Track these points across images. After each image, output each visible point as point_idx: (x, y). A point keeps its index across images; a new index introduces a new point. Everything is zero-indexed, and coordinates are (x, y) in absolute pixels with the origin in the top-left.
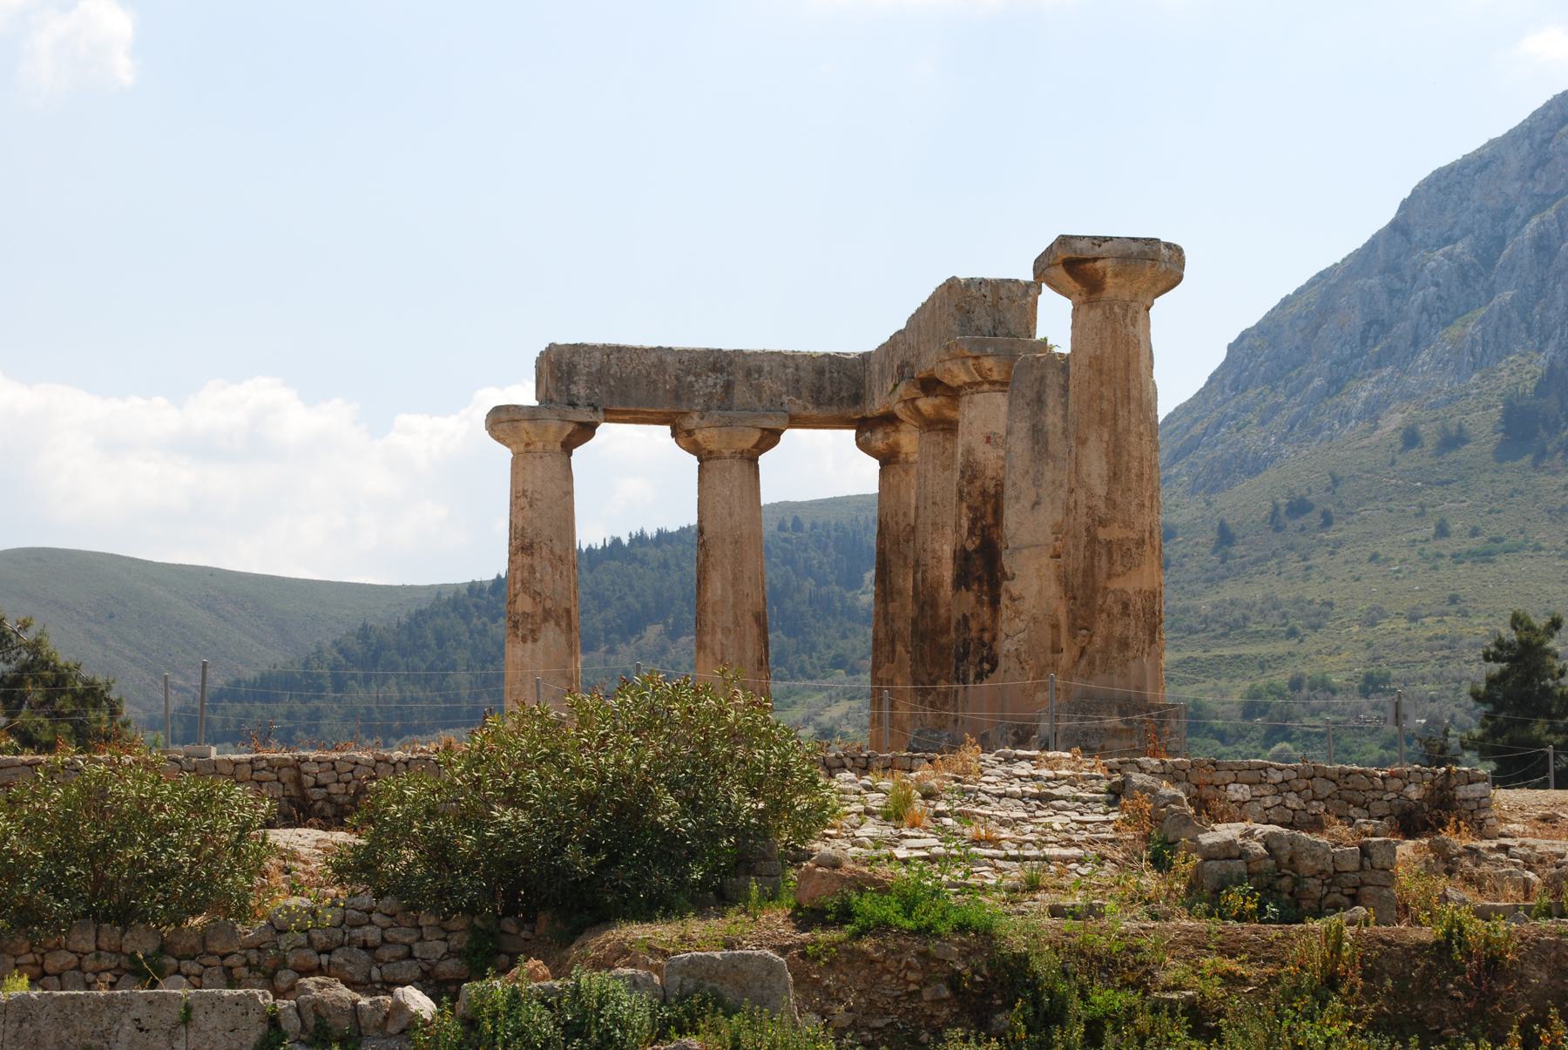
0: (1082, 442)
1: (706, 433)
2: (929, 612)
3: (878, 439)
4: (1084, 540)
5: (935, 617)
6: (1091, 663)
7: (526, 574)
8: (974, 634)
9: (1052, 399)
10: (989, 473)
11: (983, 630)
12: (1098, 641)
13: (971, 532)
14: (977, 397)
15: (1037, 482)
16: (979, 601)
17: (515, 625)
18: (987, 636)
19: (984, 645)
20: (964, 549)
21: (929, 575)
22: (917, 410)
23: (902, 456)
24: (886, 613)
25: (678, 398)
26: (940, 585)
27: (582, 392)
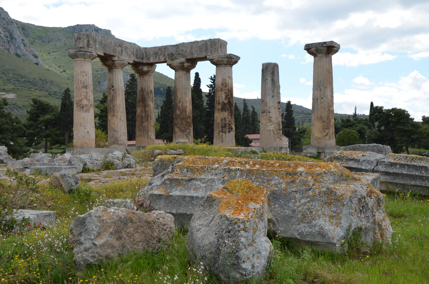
0: (326, 88)
1: (118, 62)
2: (184, 113)
3: (145, 69)
4: (327, 109)
5: (186, 115)
6: (330, 137)
7: (85, 94)
8: (227, 122)
9: (276, 73)
10: (230, 86)
11: (229, 121)
12: (331, 132)
13: (226, 99)
14: (227, 68)
15: (273, 91)
16: (228, 114)
17: (83, 107)
18: (230, 123)
19: (229, 125)
20: (224, 102)
21: (184, 105)
22: (183, 65)
23: (149, 74)
24: (145, 110)
25: (114, 52)
26: (187, 107)
27: (98, 47)
